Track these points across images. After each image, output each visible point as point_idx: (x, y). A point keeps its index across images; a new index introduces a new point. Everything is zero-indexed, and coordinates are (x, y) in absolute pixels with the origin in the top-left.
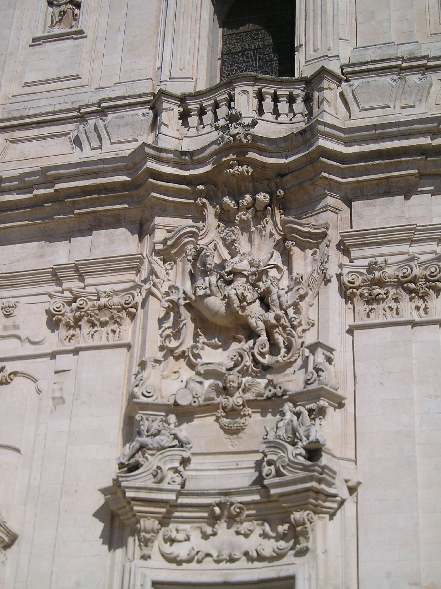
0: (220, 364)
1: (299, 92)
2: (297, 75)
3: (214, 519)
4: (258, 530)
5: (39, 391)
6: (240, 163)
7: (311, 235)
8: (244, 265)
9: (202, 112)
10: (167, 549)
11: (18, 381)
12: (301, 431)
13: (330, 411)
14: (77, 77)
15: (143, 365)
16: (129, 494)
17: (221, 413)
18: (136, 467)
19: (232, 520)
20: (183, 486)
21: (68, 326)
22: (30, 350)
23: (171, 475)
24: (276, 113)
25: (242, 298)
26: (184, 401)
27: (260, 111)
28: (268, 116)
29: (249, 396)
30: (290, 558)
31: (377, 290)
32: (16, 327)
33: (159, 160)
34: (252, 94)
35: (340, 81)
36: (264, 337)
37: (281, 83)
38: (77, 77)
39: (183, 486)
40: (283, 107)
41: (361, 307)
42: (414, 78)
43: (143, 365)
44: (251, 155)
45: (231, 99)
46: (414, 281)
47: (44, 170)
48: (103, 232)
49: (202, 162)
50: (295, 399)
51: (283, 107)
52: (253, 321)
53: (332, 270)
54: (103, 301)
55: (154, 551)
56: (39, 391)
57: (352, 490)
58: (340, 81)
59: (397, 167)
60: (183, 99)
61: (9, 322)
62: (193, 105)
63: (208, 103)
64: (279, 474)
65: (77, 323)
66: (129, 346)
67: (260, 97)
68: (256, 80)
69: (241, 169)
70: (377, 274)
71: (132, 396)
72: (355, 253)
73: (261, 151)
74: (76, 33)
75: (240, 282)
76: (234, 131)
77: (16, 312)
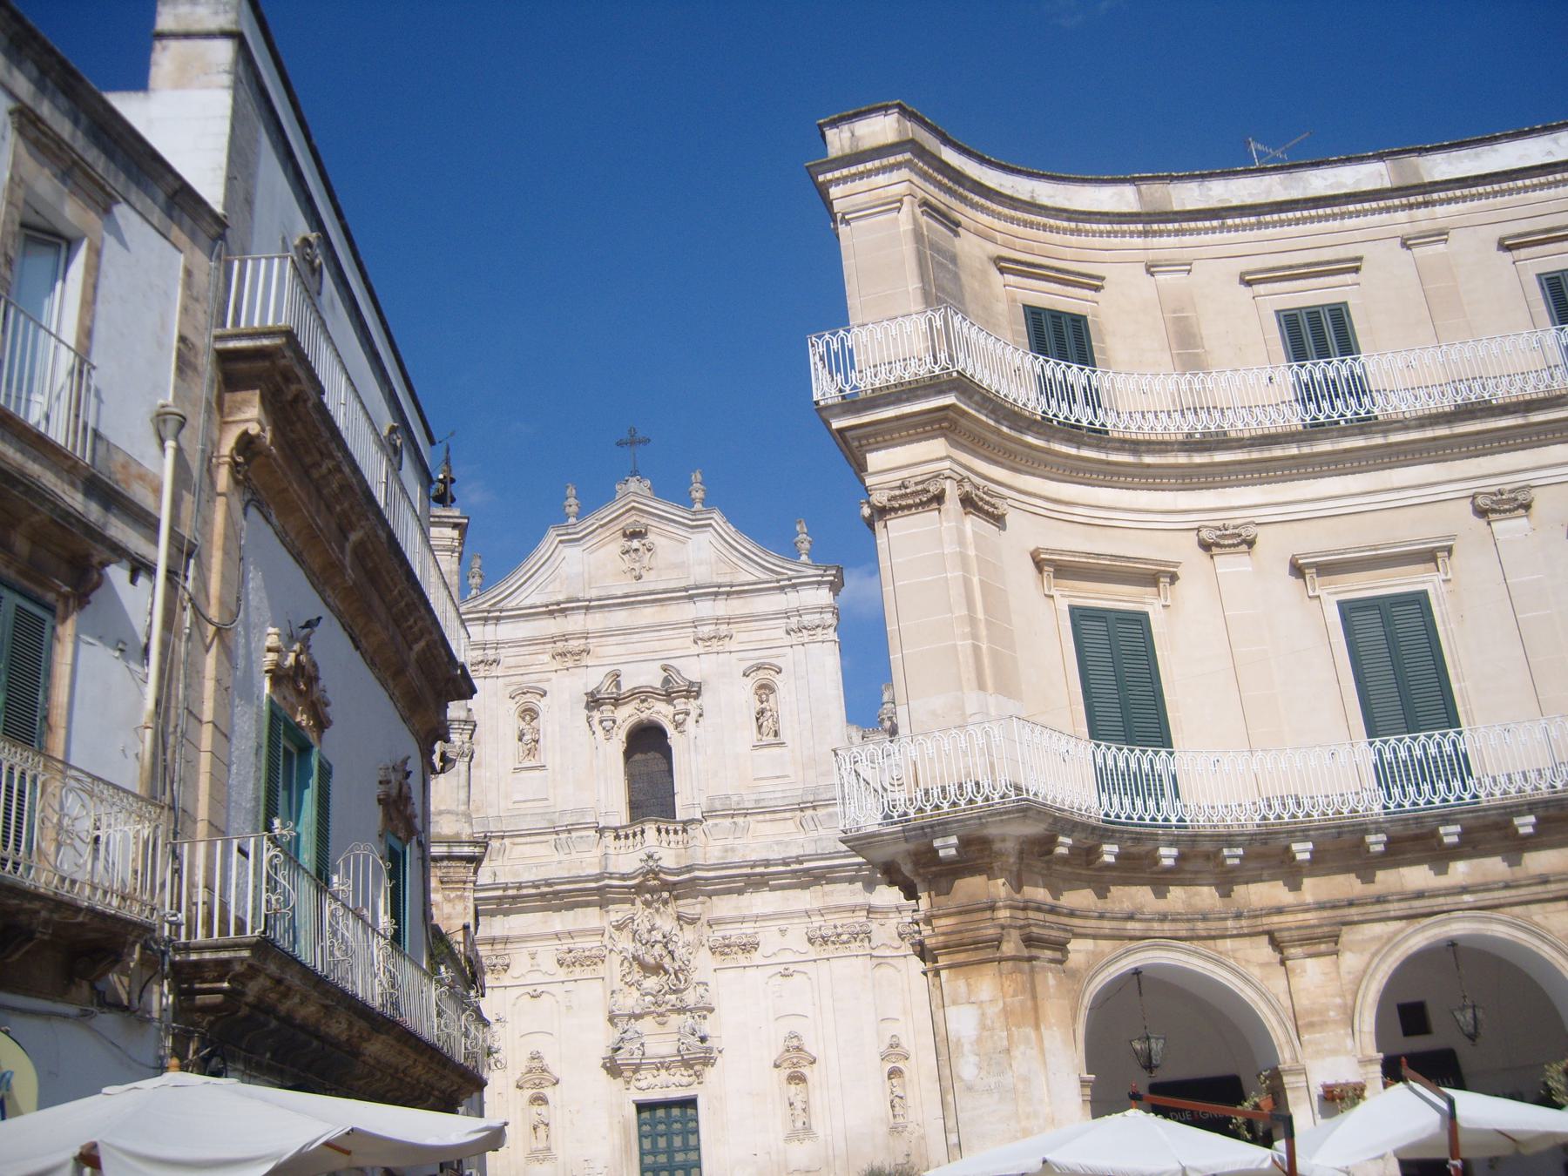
0: (652, 989)
1: (679, 827)
2: (678, 819)
3: (658, 1069)
4: (679, 1073)
5: (557, 1002)
6: (654, 879)
7: (692, 919)
8: (660, 937)
10: (639, 1084)
11: (544, 995)
12: (697, 1028)
13: (708, 1015)
14: (547, 799)
16: (618, 1062)
17: (655, 1015)
18: (619, 1049)
19: (668, 1069)
20: (643, 1054)
21: (568, 966)
23: (636, 1051)
25: (661, 956)
26: (637, 1012)
28: (664, 844)
29: (669, 1007)
30: (695, 1085)
31: (727, 950)
32: (538, 965)
33: (610, 878)
34: (655, 829)
35: (701, 822)
36: (673, 976)
37: (669, 822)
39: (643, 1054)
42: (740, 820)
44: (662, 875)
45: (643, 832)
46: (744, 945)
47: (546, 880)
48: (580, 909)
49: (634, 878)
50: (691, 1011)
52: (667, 966)
54: (587, 953)
55: (632, 1087)
56: (557, 1002)
57: (720, 1052)
58: (701, 822)
59: (734, 882)
60: (616, 829)
61: (534, 962)
62: (622, 833)
63: (630, 832)
64: (688, 1049)
67: (659, 830)
68: (656, 821)
69: (656, 882)
70: (727, 942)
72: (715, 927)
73: (665, 873)
75: (658, 946)
76: (651, 863)
77: (537, 956)
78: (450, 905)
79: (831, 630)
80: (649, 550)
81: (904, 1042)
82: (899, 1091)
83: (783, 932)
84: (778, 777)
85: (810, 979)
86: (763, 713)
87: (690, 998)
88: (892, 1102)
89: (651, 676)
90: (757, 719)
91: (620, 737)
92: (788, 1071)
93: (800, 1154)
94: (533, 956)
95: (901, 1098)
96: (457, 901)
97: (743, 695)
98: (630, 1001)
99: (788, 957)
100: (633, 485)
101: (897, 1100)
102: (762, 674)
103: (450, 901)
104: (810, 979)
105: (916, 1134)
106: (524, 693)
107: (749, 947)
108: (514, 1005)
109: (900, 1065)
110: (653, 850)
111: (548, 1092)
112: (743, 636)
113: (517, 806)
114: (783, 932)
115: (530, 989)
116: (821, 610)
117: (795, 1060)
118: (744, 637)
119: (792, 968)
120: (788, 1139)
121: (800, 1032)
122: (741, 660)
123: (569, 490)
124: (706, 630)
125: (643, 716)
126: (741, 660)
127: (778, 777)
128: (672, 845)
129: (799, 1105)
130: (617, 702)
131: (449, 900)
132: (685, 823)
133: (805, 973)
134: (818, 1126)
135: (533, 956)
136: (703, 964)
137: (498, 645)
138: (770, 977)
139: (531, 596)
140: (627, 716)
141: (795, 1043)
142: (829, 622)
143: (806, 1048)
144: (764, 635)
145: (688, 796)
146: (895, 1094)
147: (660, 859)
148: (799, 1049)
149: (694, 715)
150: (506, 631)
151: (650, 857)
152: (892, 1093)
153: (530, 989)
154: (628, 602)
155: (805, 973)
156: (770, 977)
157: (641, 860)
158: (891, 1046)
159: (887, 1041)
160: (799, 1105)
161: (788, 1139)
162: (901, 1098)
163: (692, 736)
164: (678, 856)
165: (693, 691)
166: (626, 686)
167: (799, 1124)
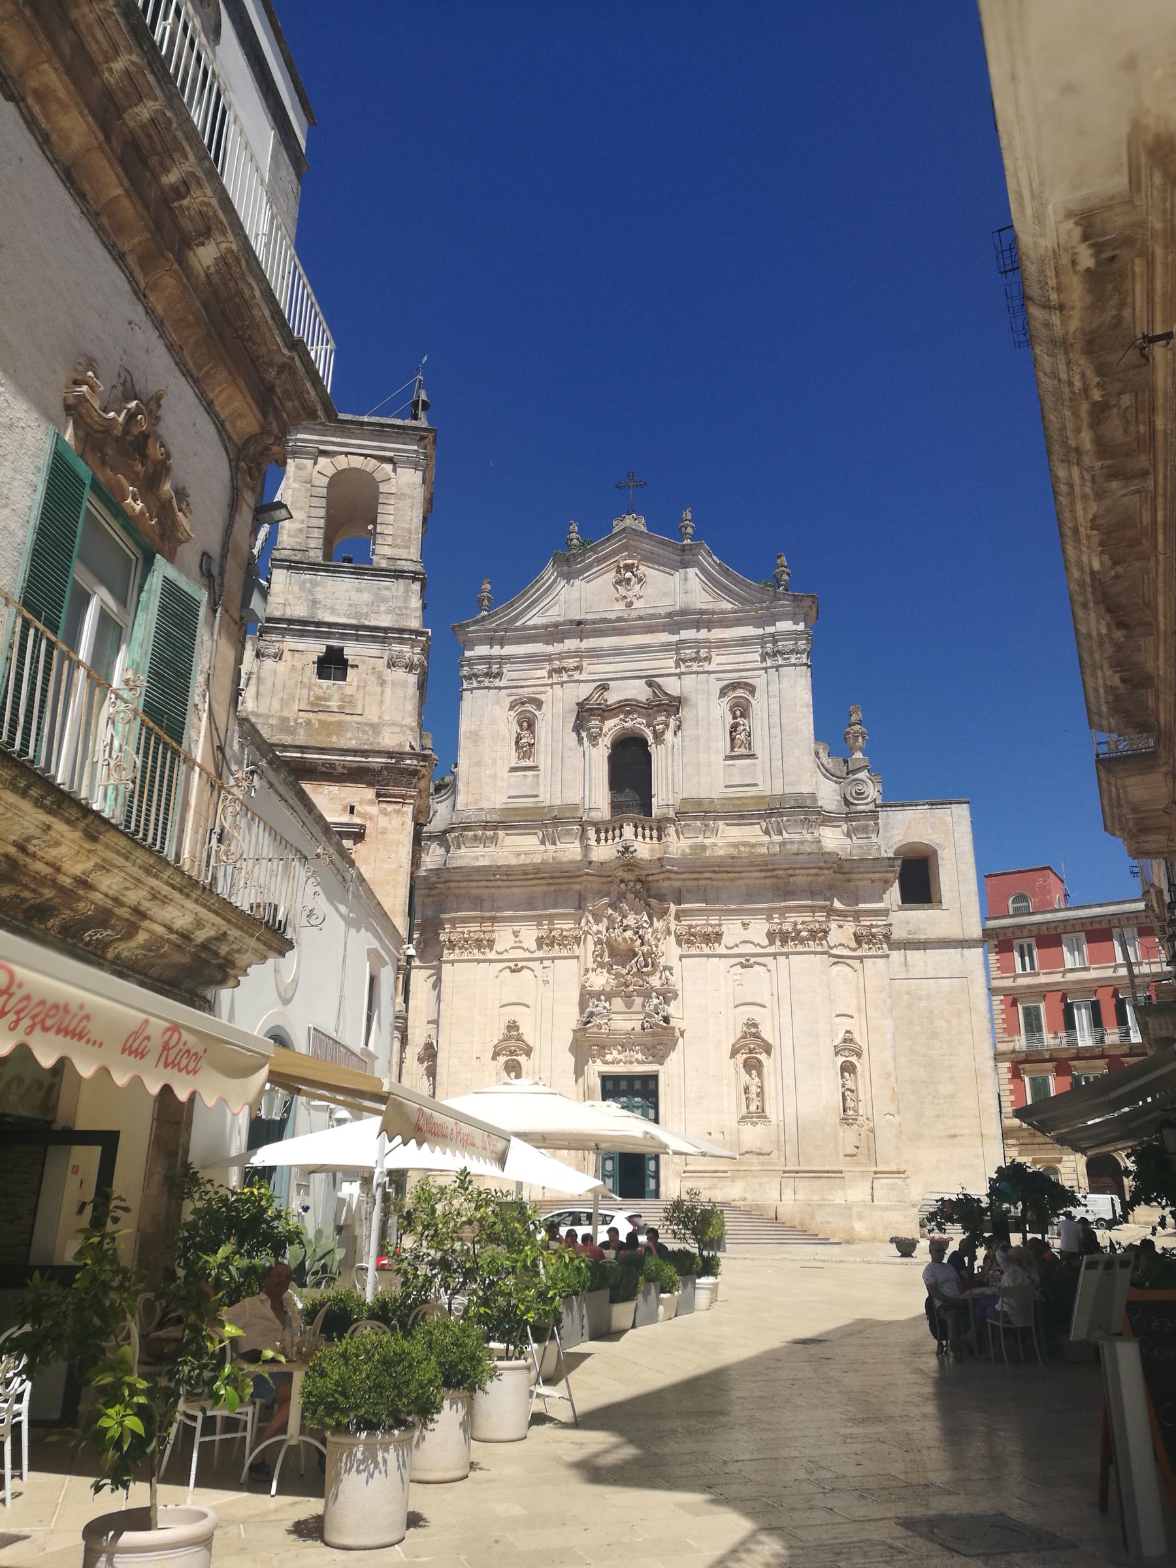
1: (655, 826)
9: (607, 831)
14: (537, 796)
15: (587, 970)
22: (528, 955)
24: (644, 837)
27: (636, 835)
28: (640, 838)
32: (521, 942)
38: (537, 796)
40: (647, 832)
41: (685, 946)
43: (587, 970)
45: (621, 827)
51: (647, 832)
53: (673, 927)
54: (564, 933)
61: (517, 939)
64: (651, 1028)
65: (552, 944)
66: (578, 958)
71: (583, 987)
74: (534, 767)
78: (387, 819)
79: (805, 656)
80: (640, 580)
81: (857, 1037)
82: (850, 1084)
83: (745, 926)
84: (747, 785)
85: (769, 971)
86: (736, 727)
87: (655, 981)
88: (843, 1094)
89: (638, 691)
90: (731, 732)
91: (605, 743)
92: (745, 1056)
93: (753, 1136)
94: (516, 934)
95: (852, 1091)
96: (394, 815)
97: (719, 712)
98: (600, 980)
99: (749, 949)
100: (629, 521)
101: (848, 1093)
102: (739, 693)
103: (386, 814)
104: (769, 971)
105: (866, 1127)
106: (523, 703)
107: (714, 938)
108: (497, 977)
109: (854, 1059)
110: (629, 843)
111: (522, 1059)
112: (719, 661)
113: (511, 800)
114: (745, 926)
115: (512, 965)
116: (795, 636)
117: (752, 1046)
118: (723, 659)
119: (752, 960)
120: (743, 1119)
121: (758, 1021)
122: (718, 680)
123: (571, 527)
124: (689, 653)
125: (627, 725)
126: (718, 680)
127: (747, 785)
128: (647, 840)
129: (754, 1090)
130: (605, 712)
131: (384, 813)
132: (659, 821)
133: (765, 966)
134: (770, 1110)
135: (516, 934)
136: (669, 951)
137: (502, 660)
138: (731, 967)
139: (535, 618)
140: (612, 726)
141: (753, 1030)
142: (804, 647)
143: (763, 1035)
144: (741, 658)
145: (663, 796)
146: (847, 1087)
147: (635, 851)
148: (756, 1036)
149: (672, 723)
150: (509, 650)
151: (627, 849)
152: (843, 1086)
153: (512, 965)
154: (617, 627)
155: (765, 966)
156: (731, 967)
157: (618, 851)
158: (845, 1041)
159: (841, 1036)
160: (754, 1090)
161: (743, 1119)
162: (852, 1091)
163: (670, 745)
164: (652, 850)
165: (673, 705)
166: (612, 698)
167: (753, 1108)
